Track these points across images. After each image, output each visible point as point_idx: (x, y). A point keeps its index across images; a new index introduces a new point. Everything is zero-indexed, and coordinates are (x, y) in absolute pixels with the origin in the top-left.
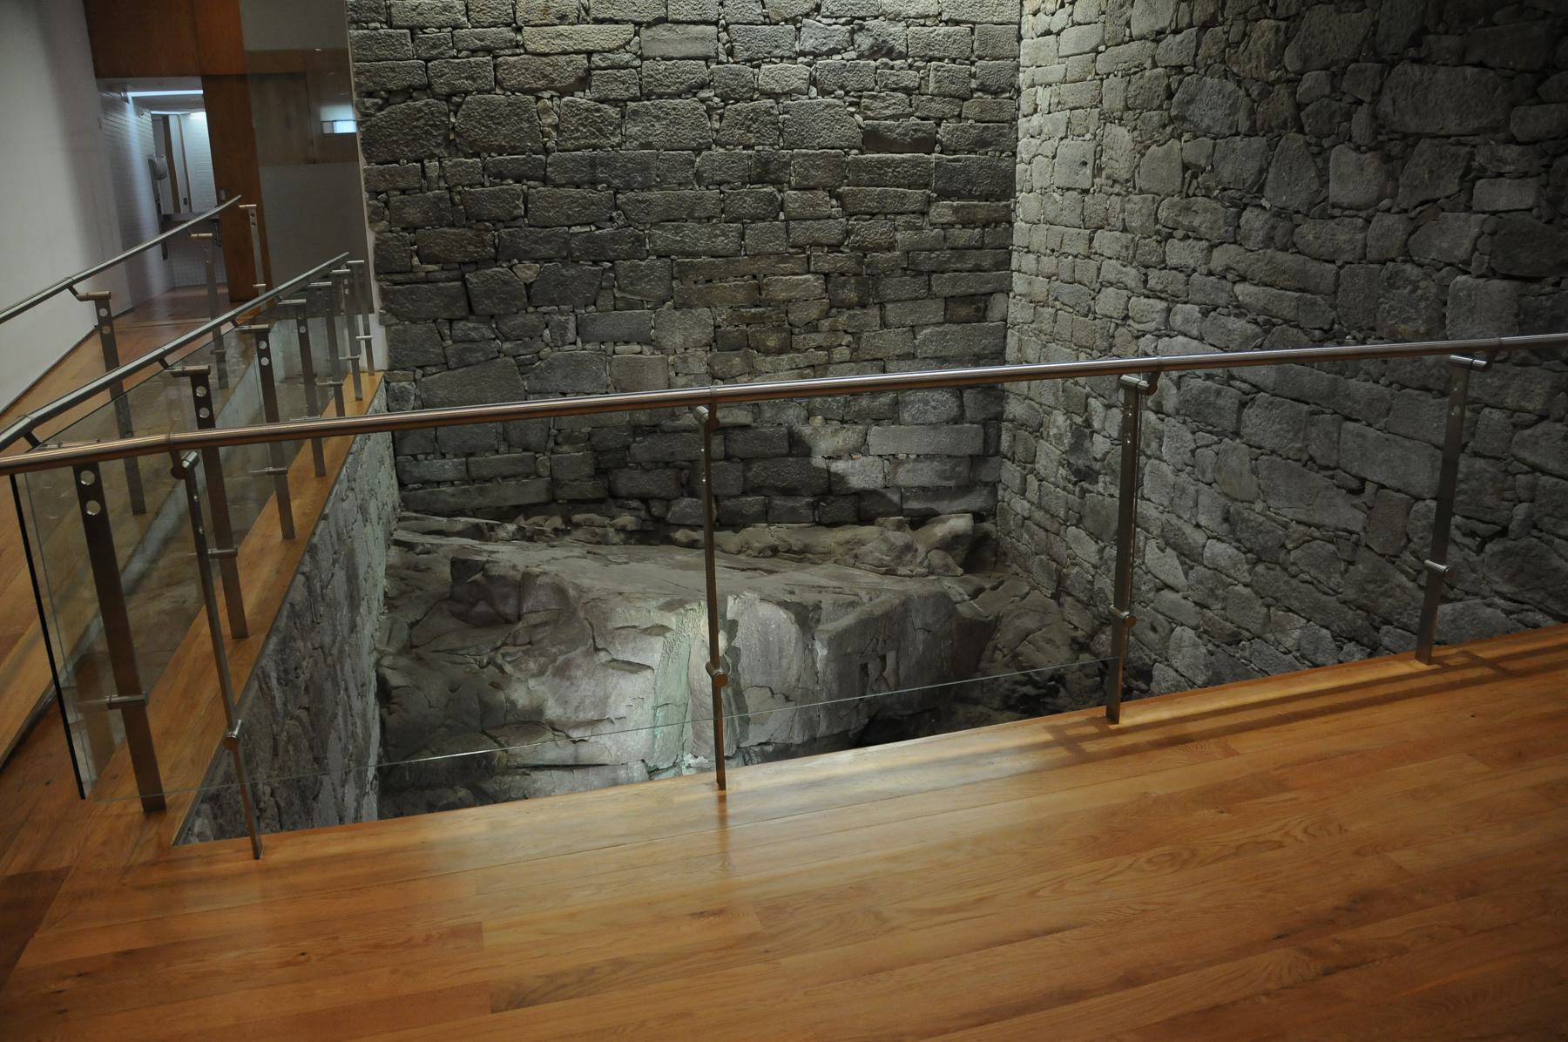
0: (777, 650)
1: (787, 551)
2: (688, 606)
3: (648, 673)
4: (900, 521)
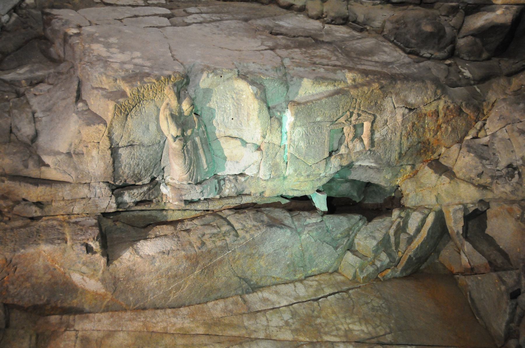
0: (246, 114)
1: (354, 22)
2: (145, 80)
3: (101, 127)
4: (453, 7)
